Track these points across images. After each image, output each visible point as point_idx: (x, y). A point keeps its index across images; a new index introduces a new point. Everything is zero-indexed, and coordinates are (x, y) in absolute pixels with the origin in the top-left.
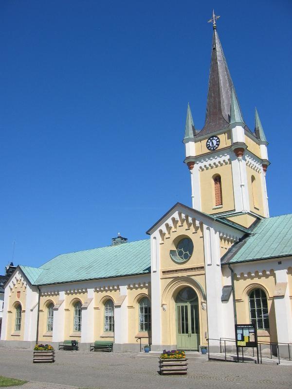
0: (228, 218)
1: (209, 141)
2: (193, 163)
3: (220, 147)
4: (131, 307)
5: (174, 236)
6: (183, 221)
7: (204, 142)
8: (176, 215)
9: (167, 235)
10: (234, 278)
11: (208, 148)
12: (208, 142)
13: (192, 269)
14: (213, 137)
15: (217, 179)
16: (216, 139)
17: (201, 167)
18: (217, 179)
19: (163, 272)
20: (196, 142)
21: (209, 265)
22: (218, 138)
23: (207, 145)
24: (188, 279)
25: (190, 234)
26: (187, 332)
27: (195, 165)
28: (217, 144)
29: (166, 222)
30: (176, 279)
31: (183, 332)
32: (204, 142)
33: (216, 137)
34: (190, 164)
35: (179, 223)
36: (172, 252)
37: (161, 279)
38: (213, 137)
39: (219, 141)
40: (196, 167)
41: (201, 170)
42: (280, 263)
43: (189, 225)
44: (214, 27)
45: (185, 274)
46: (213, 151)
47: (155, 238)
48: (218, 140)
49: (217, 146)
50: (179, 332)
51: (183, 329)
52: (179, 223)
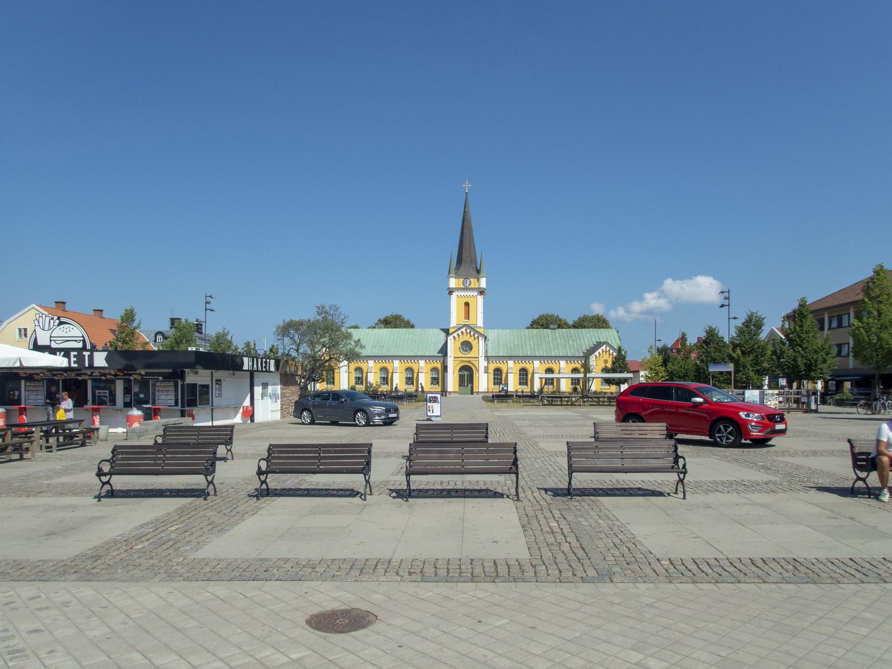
0: (475, 329)
2: (453, 292)
3: (470, 287)
4: (427, 373)
5: (462, 340)
6: (467, 333)
7: (461, 280)
8: (463, 330)
9: (457, 339)
10: (488, 362)
11: (463, 285)
13: (471, 357)
15: (467, 304)
17: (458, 295)
18: (467, 304)
20: (455, 278)
24: (469, 362)
25: (471, 340)
26: (464, 386)
27: (454, 293)
30: (463, 361)
31: (462, 386)
34: (451, 293)
35: (465, 334)
36: (459, 348)
40: (455, 294)
42: (510, 359)
43: (471, 336)
45: (468, 359)
46: (466, 289)
50: (460, 386)
51: (461, 383)
52: (465, 334)
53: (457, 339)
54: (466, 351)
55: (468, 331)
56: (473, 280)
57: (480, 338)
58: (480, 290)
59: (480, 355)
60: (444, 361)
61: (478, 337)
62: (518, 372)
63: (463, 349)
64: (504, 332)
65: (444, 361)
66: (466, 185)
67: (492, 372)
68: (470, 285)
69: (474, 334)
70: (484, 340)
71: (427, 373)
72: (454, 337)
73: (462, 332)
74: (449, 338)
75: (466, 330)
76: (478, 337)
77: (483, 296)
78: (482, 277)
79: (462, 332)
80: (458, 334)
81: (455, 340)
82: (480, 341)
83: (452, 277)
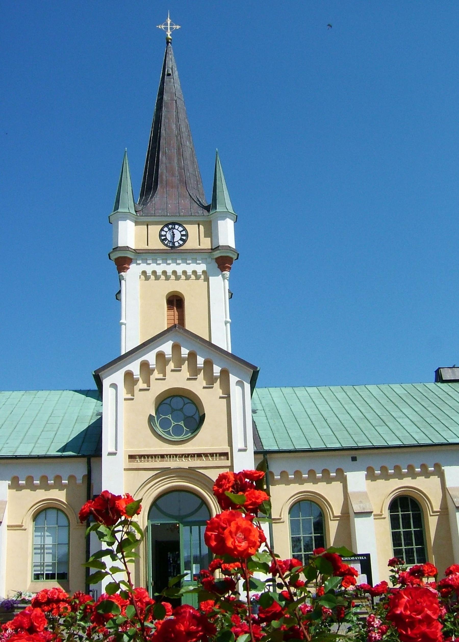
1: (166, 229)
3: (188, 246)
4: (19, 527)
7: (155, 230)
11: (162, 241)
12: (162, 230)
13: (199, 455)
14: (174, 224)
16: (181, 229)
17: (144, 273)
19: (131, 457)
20: (137, 223)
21: (240, 450)
22: (185, 229)
23: (161, 236)
27: (133, 267)
28: (181, 239)
29: (144, 358)
30: (165, 472)
32: (155, 230)
33: (180, 225)
36: (151, 418)
37: (125, 469)
38: (174, 224)
39: (187, 235)
41: (143, 277)
42: (354, 459)
44: (167, 39)
45: (185, 464)
47: (114, 386)
48: (184, 233)
49: (181, 242)
53: (141, 385)
54: (178, 431)
55: (185, 352)
56: (192, 229)
57: (233, 379)
58: (217, 254)
59: (238, 443)
60: (89, 478)
61: (225, 373)
62: (386, 513)
63: (165, 424)
64: (301, 392)
65: (89, 478)
66: (171, 29)
67: (286, 517)
68: (184, 241)
69: (208, 364)
70: (247, 386)
71: (19, 527)
72: (129, 375)
73: (160, 355)
74: (106, 383)
75: (176, 348)
76: (225, 373)
77: (227, 273)
78: (224, 216)
79: (160, 355)
80: (145, 365)
81: (131, 391)
82: (235, 390)
83: (125, 217)
